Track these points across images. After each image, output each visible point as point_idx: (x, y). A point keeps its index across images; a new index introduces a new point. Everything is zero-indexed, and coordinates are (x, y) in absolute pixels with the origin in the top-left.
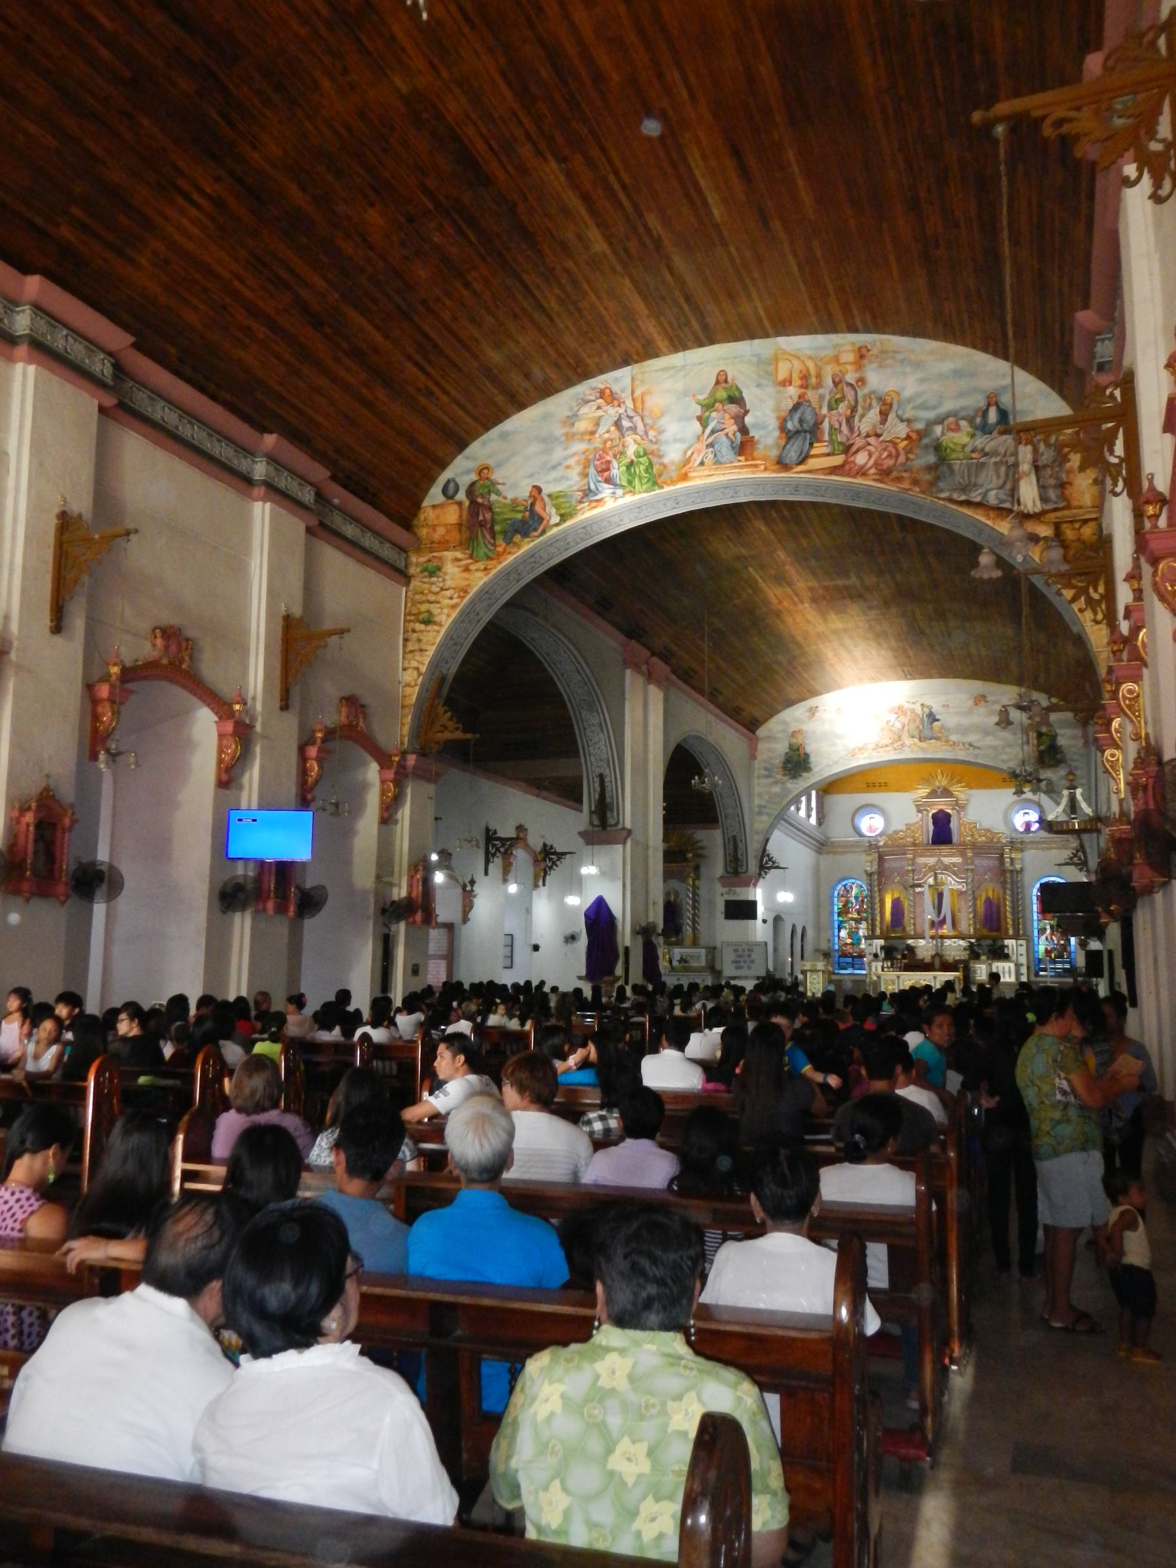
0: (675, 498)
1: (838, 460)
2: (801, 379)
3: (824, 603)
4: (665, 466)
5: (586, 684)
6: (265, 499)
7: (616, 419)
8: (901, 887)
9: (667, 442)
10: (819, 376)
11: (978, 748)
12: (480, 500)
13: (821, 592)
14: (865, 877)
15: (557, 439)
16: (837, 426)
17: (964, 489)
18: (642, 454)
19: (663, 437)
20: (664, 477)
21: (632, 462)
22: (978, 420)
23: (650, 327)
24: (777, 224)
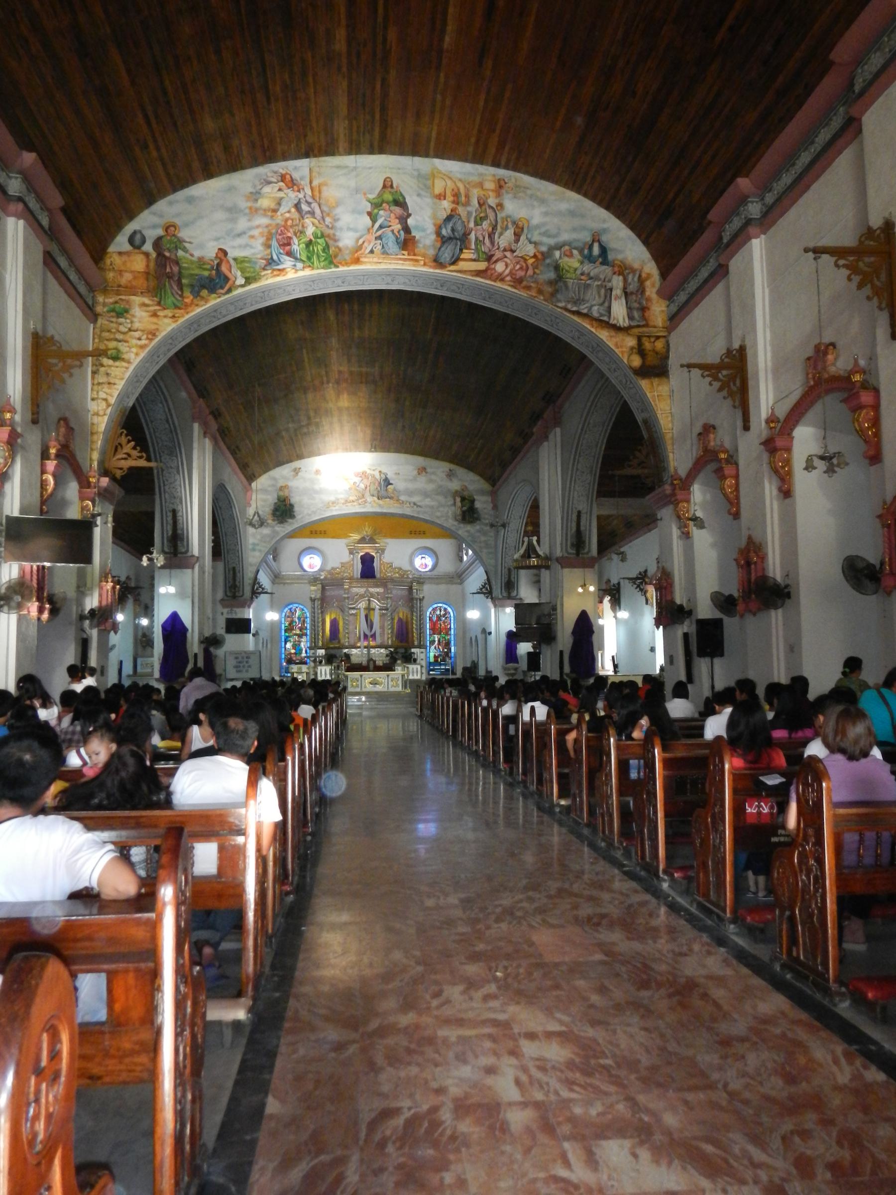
0: (343, 278)
1: (482, 266)
2: (454, 196)
3: (344, 385)
4: (340, 249)
5: (171, 432)
6: (18, 216)
7: (296, 202)
8: (338, 611)
9: (341, 229)
10: (467, 196)
11: (420, 506)
12: (167, 254)
13: (346, 376)
15: (241, 211)
16: (481, 239)
17: (576, 302)
18: (319, 235)
19: (339, 224)
20: (339, 258)
21: (311, 240)
22: (586, 252)
23: (341, 128)
24: (489, 63)
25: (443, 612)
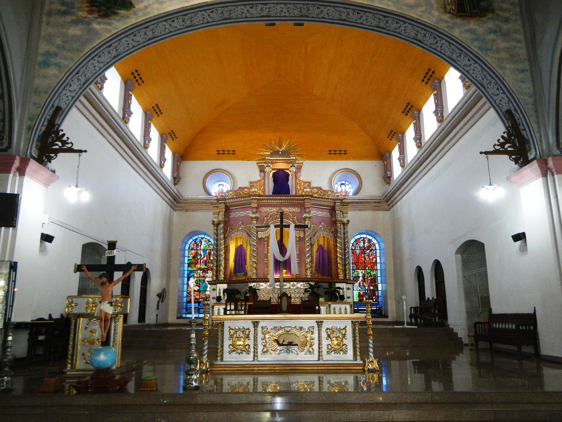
8: (245, 235)
14: (211, 229)
25: (366, 244)
